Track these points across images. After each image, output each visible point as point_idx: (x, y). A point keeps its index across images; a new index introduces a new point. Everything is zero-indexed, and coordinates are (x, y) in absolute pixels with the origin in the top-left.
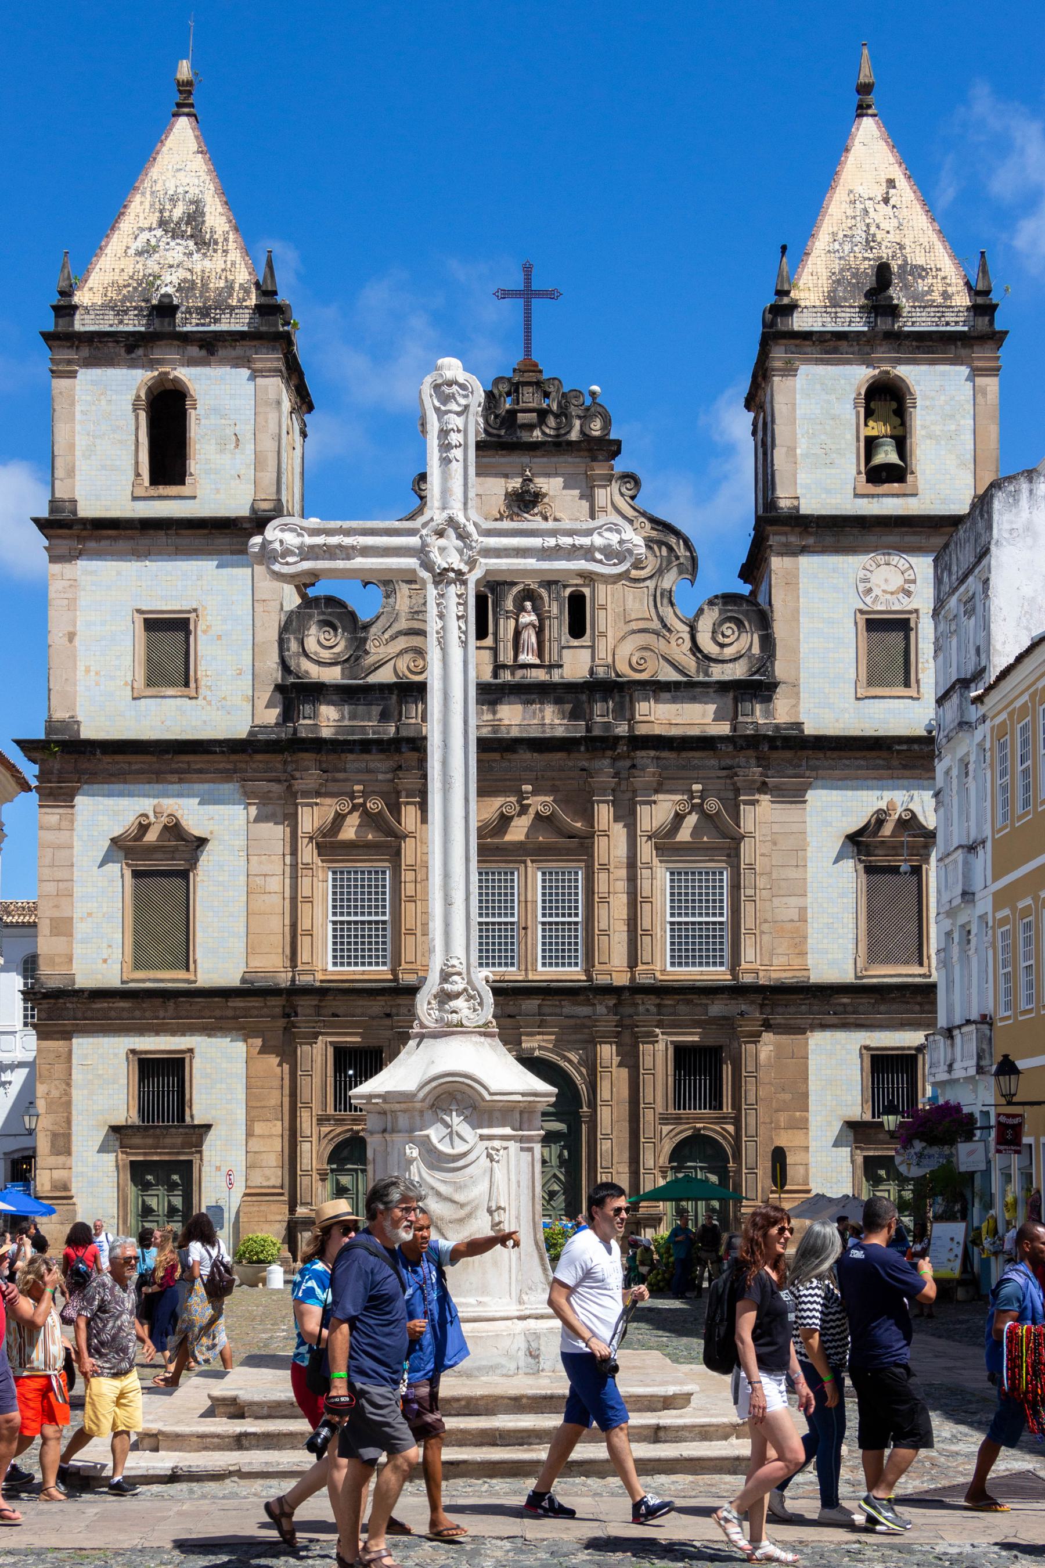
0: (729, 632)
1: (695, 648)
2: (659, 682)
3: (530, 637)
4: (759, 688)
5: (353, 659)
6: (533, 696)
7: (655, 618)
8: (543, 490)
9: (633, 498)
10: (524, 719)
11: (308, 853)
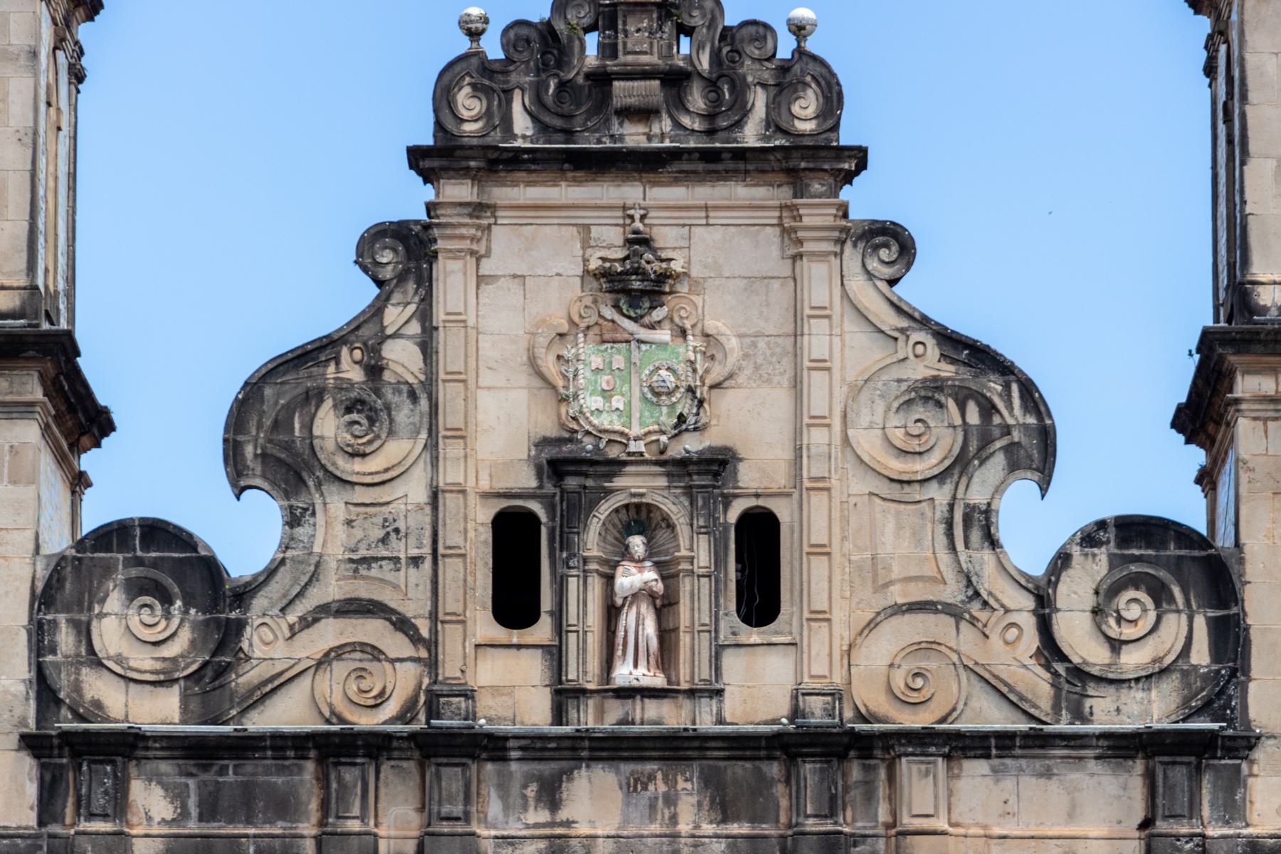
0: (1133, 612)
1: (1050, 649)
2: (958, 735)
3: (641, 624)
5: (212, 675)
6: (650, 767)
7: (950, 575)
8: (677, 266)
9: (892, 282)
10: (626, 822)
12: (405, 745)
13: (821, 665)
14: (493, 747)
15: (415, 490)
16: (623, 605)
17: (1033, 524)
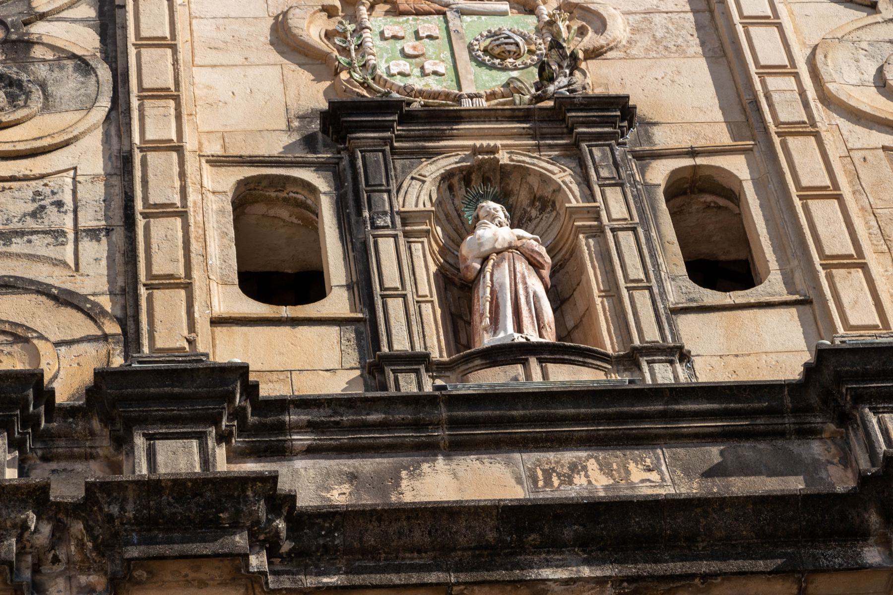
12: (80, 426)
15: (90, 157)
16: (481, 271)
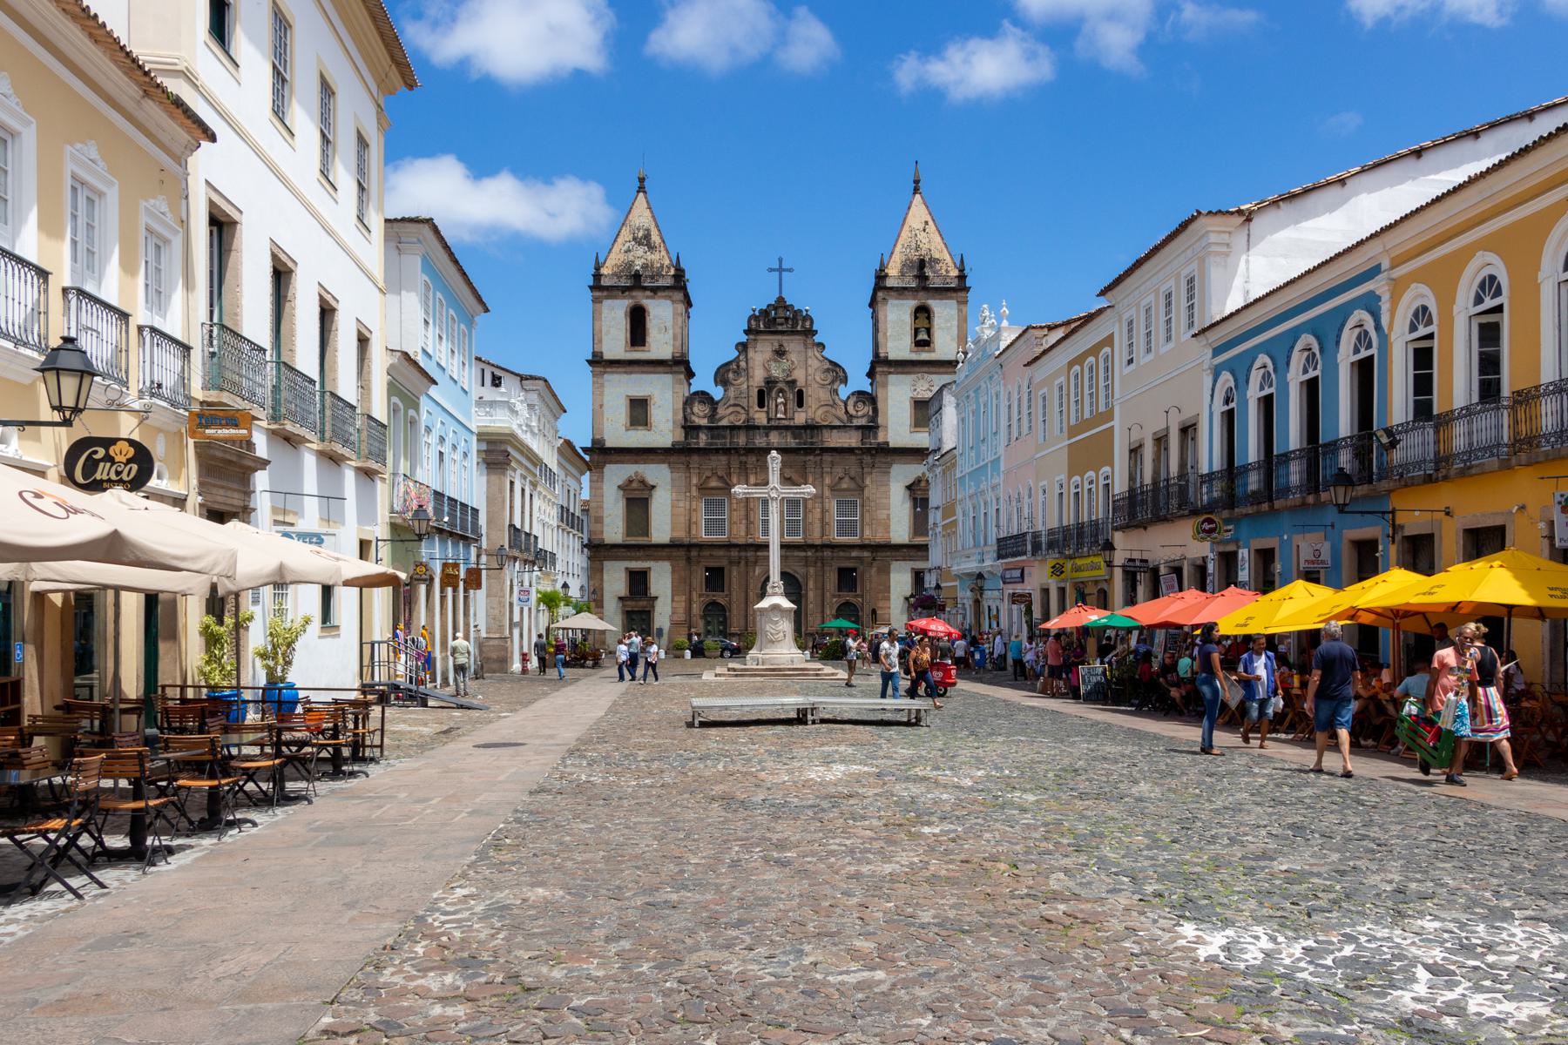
4: (871, 428)
5: (713, 416)
11: (694, 492)
13: (810, 415)
14: (758, 428)
17: (844, 392)
